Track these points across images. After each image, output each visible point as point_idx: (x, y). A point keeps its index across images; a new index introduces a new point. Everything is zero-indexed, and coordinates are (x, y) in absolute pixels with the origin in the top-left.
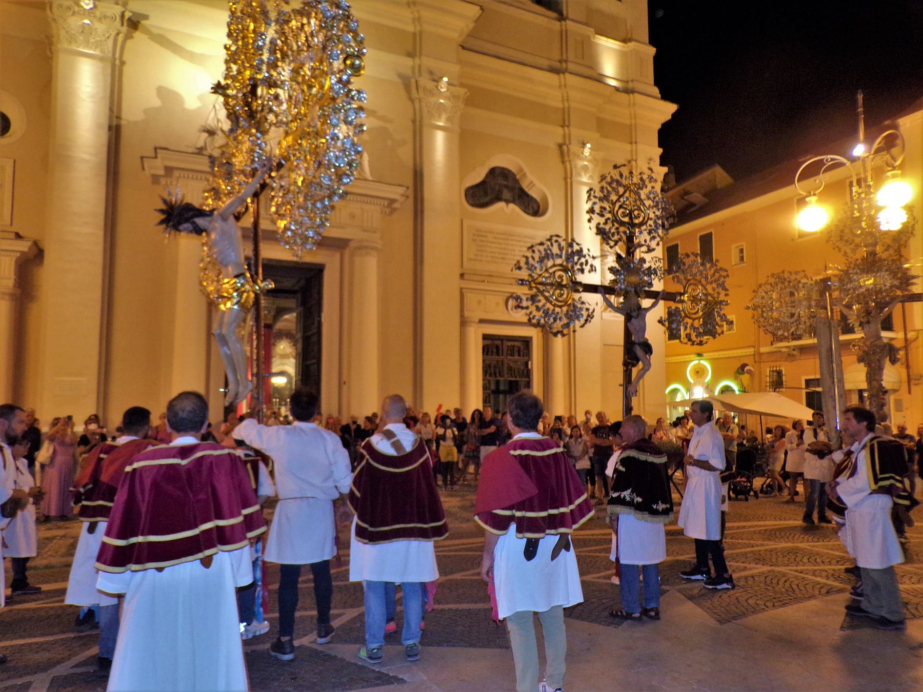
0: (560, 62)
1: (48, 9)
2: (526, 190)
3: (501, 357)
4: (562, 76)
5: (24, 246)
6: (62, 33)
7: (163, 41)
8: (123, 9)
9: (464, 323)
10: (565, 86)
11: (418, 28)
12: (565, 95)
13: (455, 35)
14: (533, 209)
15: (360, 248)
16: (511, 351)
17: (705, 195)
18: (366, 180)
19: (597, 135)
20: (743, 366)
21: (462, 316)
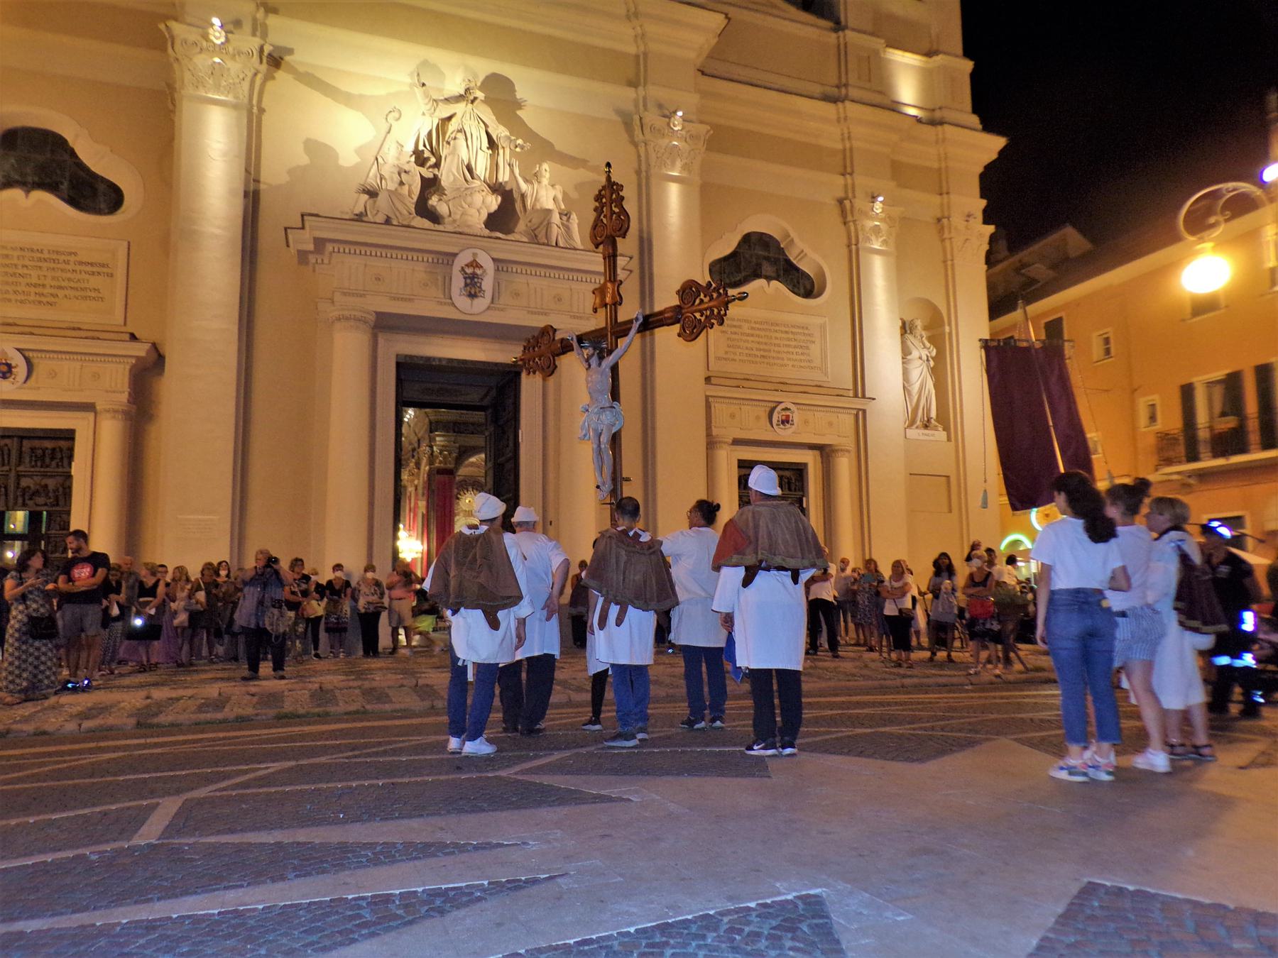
2: (795, 262)
4: (840, 105)
5: (140, 350)
6: (187, 76)
7: (311, 80)
8: (262, 42)
9: (712, 444)
10: (846, 119)
11: (642, 48)
12: (846, 131)
13: (692, 55)
14: (805, 287)
17: (1054, 267)
18: (575, 249)
19: (892, 184)
21: (709, 434)
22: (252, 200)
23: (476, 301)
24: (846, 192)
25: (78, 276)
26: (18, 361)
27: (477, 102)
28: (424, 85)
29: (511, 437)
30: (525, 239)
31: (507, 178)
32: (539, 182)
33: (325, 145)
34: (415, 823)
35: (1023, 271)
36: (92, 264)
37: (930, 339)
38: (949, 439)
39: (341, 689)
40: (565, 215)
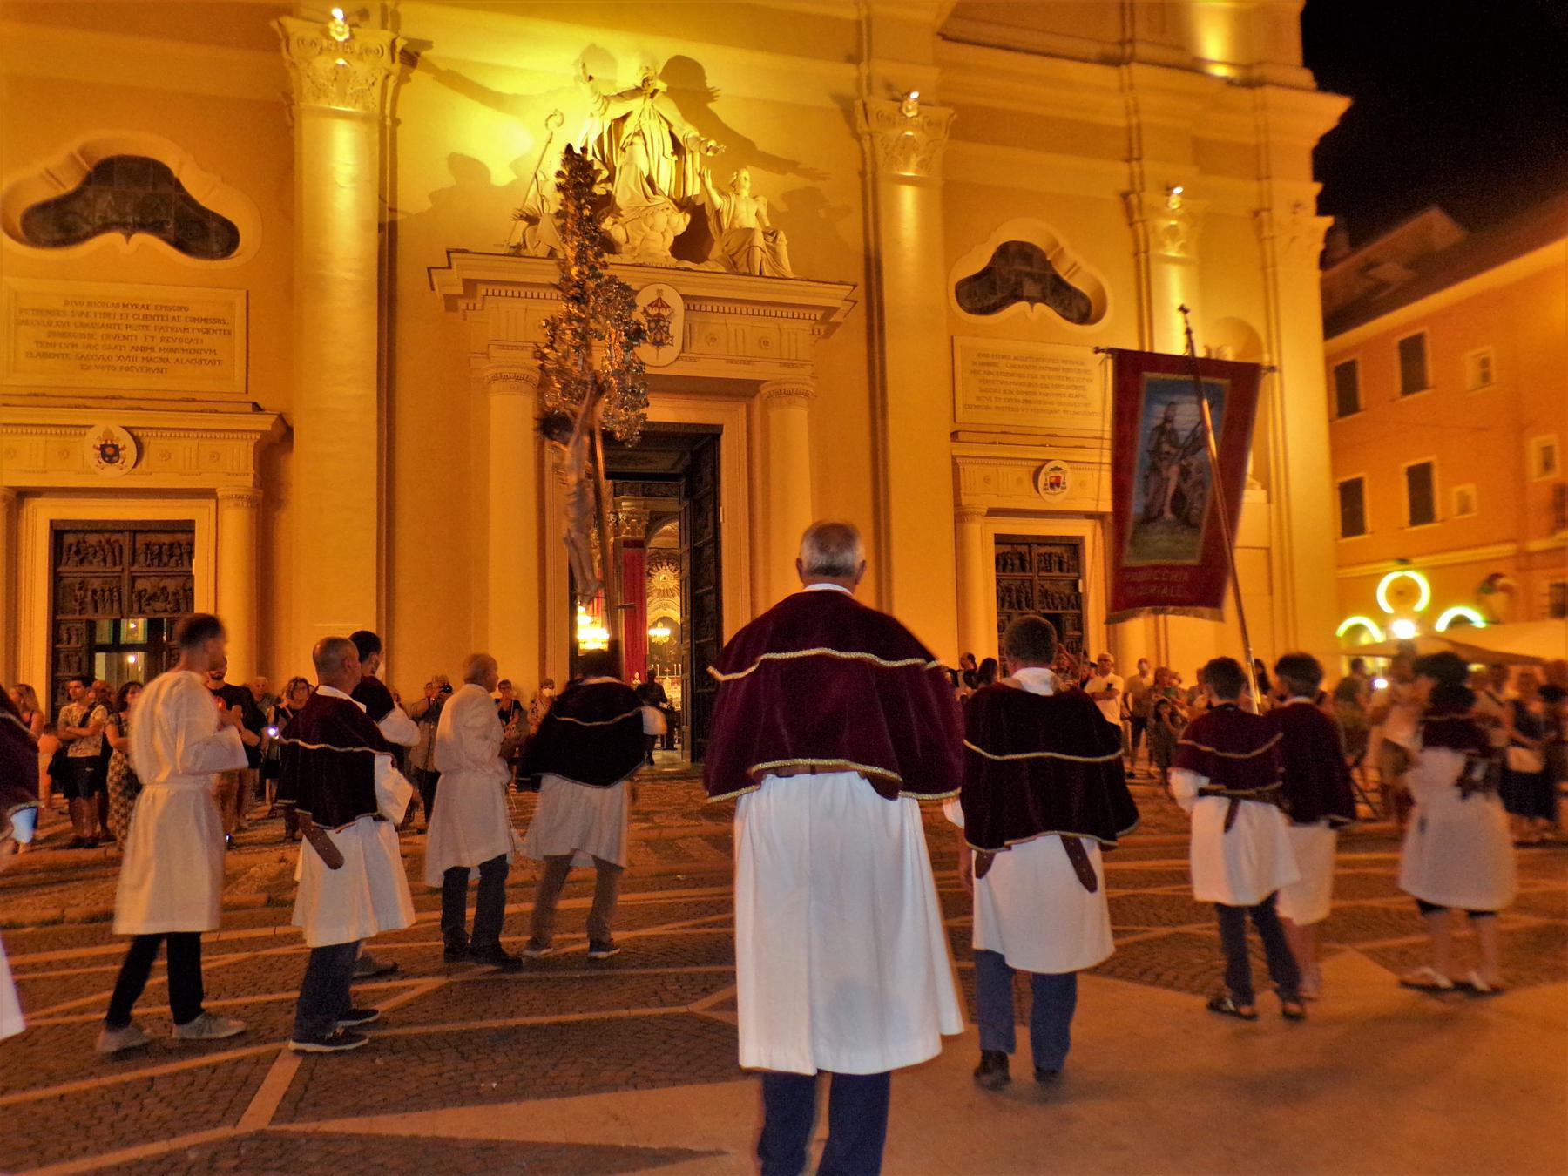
0: (1122, 43)
1: (284, 49)
2: (1065, 278)
4: (1124, 68)
5: (264, 423)
6: (307, 85)
7: (457, 81)
8: (393, 36)
9: (961, 516)
10: (1131, 87)
11: (864, 12)
12: (1131, 103)
15: (778, 394)
16: (1047, 563)
17: (1412, 265)
18: (785, 278)
20: (1495, 576)
21: (957, 504)
22: (388, 233)
23: (663, 350)
25: (189, 335)
26: (125, 441)
27: (657, 95)
28: (591, 78)
29: (711, 514)
30: (722, 269)
31: (697, 192)
34: (582, 1105)
35: (1371, 273)
36: (206, 320)
38: (1269, 501)
40: (771, 234)
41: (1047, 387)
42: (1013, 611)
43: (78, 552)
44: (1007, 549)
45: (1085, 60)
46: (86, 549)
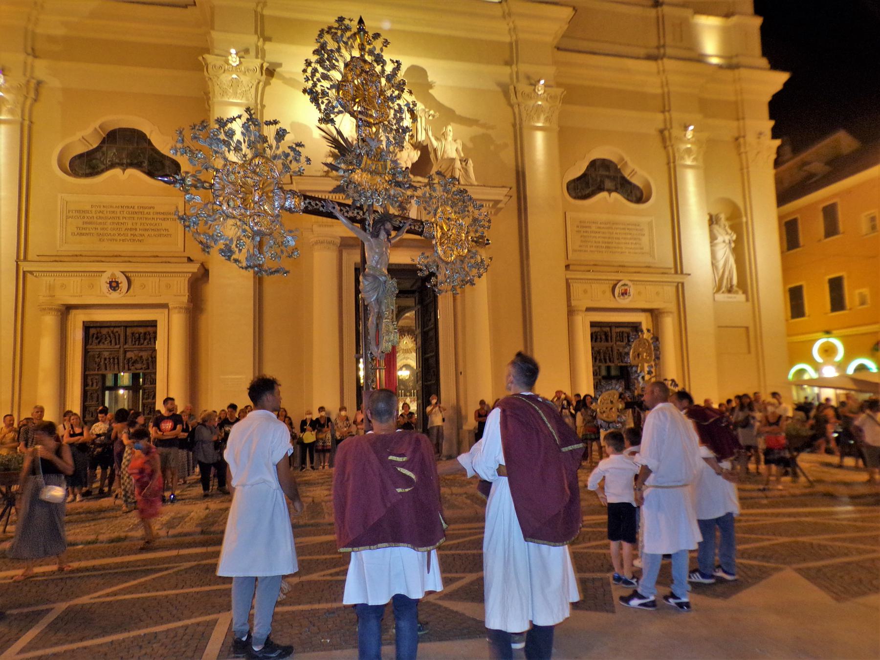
0: (658, 48)
2: (628, 178)
3: (609, 344)
4: (660, 62)
5: (194, 268)
6: (217, 88)
8: (263, 61)
9: (571, 312)
10: (664, 71)
11: (514, 38)
12: (664, 79)
13: (549, 39)
14: (636, 196)
16: (621, 337)
17: (829, 163)
21: (569, 305)
24: (665, 125)
26: (122, 279)
29: (433, 314)
31: (424, 138)
32: (446, 139)
33: (306, 126)
37: (732, 227)
38: (747, 300)
39: (326, 502)
40: (464, 161)
41: (619, 239)
42: (600, 364)
43: (97, 338)
44: (596, 329)
45: (638, 58)
46: (101, 336)
